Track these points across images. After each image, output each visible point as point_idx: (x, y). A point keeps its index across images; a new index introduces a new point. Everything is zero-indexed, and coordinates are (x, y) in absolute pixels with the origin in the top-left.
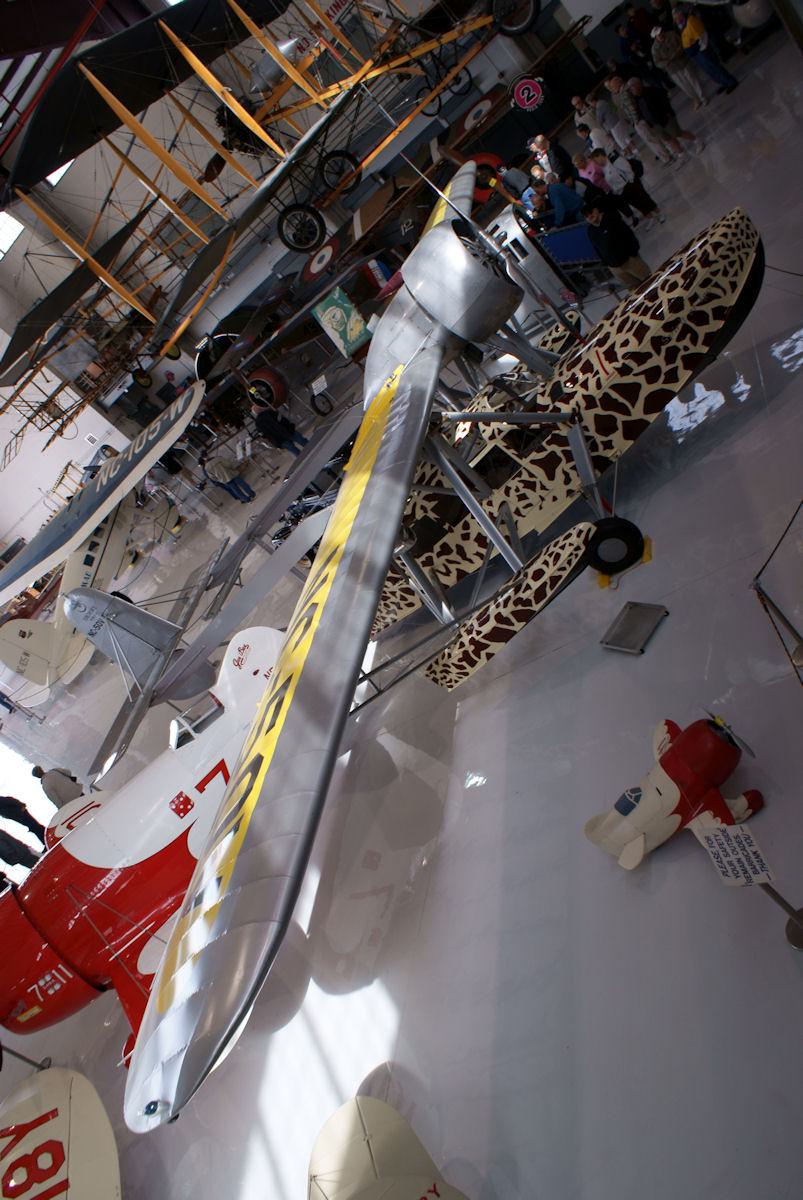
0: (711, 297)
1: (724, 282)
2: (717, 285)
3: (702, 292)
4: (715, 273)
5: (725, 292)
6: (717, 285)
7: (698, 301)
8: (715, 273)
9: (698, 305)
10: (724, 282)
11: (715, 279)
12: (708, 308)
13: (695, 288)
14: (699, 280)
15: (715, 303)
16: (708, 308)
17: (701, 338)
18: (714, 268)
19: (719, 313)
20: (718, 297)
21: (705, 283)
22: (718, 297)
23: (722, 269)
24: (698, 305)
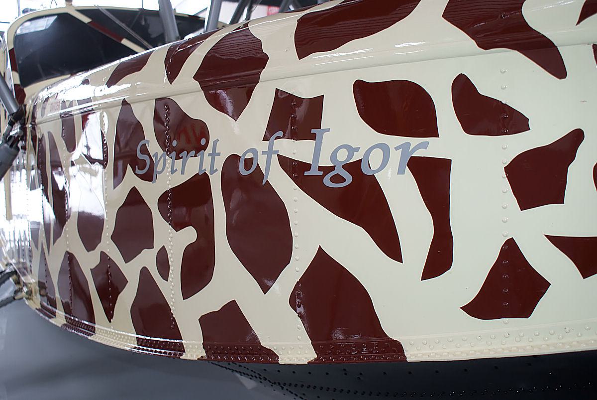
0: (358, 199)
1: (487, 215)
2: (433, 178)
3: (346, 134)
4: (483, 114)
5: (439, 260)
6: (433, 178)
7: (299, 150)
8: (483, 114)
9: (295, 169)
10: (487, 215)
11: (450, 140)
12: (317, 230)
13: (331, 76)
14: (381, 55)
15: (350, 246)
16: (317, 230)
17: (210, 299)
18: (504, 75)
19: (331, 297)
20: (390, 245)
21: (394, 107)
22: (390, 245)
23: (541, 135)
24: (295, 169)
